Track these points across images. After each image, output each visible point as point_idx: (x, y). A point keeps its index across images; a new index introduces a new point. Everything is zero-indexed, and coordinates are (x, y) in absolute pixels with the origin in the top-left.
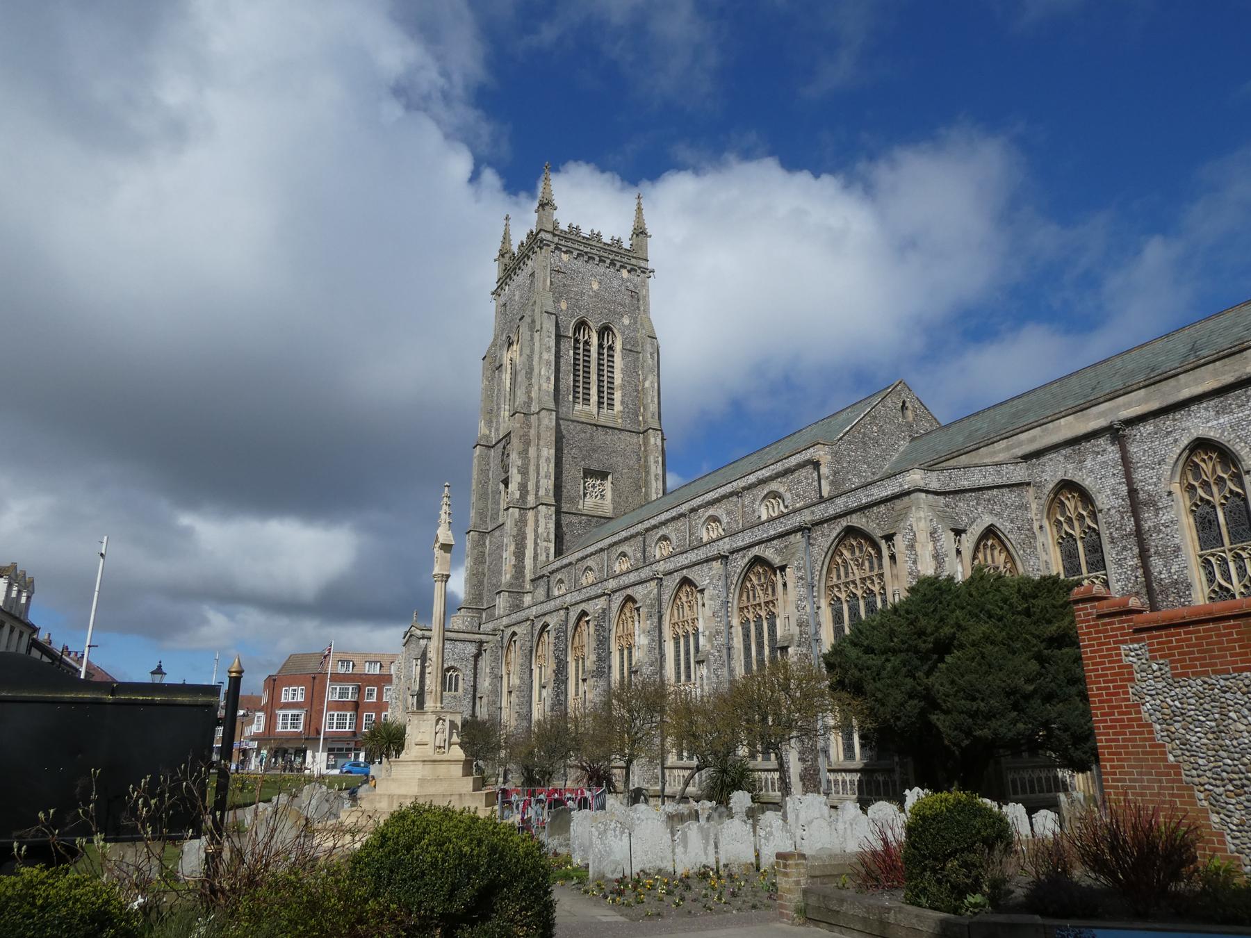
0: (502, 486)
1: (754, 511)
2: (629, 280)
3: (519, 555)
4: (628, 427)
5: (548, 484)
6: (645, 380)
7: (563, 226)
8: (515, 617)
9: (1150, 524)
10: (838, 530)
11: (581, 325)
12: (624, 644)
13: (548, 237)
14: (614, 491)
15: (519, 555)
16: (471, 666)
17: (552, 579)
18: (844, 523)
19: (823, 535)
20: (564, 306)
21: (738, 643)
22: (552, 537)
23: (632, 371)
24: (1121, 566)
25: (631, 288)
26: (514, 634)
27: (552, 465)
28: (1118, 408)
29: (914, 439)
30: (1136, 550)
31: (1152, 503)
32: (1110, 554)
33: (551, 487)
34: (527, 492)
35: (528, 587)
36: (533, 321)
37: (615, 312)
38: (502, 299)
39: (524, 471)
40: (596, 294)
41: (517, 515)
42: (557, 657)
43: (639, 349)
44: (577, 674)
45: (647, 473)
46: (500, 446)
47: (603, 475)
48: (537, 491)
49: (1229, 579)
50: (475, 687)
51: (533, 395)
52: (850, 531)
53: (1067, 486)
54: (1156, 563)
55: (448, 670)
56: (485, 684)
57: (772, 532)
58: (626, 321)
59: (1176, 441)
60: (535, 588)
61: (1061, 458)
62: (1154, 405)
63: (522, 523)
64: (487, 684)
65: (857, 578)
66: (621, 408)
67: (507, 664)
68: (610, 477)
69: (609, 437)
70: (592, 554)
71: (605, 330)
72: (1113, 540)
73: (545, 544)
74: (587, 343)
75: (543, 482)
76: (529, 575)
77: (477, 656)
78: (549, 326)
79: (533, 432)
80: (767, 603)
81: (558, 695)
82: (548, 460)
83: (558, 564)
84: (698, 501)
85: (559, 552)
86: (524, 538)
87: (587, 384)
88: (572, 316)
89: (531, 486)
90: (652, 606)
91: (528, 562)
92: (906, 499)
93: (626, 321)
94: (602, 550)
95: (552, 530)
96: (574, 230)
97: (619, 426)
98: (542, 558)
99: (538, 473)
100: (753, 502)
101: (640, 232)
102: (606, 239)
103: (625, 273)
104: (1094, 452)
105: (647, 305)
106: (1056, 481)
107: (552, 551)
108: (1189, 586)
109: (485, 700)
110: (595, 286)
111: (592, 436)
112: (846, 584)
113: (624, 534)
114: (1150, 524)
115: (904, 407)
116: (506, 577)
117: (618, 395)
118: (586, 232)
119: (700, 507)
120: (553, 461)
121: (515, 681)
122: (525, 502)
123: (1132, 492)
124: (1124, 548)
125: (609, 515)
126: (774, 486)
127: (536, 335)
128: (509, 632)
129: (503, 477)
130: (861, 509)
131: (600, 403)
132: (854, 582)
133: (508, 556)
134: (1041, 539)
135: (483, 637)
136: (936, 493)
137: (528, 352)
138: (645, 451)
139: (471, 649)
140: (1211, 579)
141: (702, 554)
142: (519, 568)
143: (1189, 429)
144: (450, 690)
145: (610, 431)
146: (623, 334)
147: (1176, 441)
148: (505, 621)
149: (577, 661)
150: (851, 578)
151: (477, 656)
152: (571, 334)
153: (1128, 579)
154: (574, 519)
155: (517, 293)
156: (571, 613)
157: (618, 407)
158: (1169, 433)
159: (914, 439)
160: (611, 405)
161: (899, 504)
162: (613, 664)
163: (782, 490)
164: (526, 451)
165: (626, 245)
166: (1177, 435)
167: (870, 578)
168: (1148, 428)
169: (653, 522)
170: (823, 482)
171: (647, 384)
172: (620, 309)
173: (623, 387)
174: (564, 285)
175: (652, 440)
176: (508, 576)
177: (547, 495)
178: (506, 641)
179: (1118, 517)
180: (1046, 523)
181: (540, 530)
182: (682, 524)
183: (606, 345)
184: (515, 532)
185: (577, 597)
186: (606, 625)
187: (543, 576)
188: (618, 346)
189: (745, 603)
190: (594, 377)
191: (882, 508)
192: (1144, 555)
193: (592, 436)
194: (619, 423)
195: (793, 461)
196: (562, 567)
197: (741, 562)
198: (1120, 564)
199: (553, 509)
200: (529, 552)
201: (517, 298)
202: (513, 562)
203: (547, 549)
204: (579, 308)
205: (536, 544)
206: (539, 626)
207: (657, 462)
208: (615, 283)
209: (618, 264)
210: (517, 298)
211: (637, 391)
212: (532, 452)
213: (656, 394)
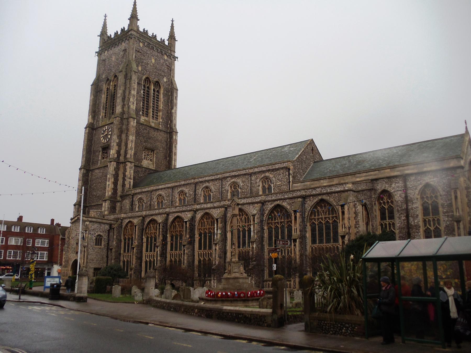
1: (256, 183)
2: (167, 60)
5: (131, 153)
7: (141, 30)
9: (410, 207)
10: (317, 200)
11: (147, 79)
13: (135, 33)
15: (115, 183)
16: (107, 235)
19: (310, 200)
20: (140, 69)
21: (266, 235)
22: (132, 177)
24: (400, 219)
25: (168, 64)
27: (133, 144)
28: (405, 170)
29: (315, 162)
30: (405, 215)
31: (411, 201)
32: (396, 215)
34: (120, 155)
35: (119, 199)
37: (161, 75)
38: (103, 57)
39: (119, 145)
41: (115, 166)
42: (163, 235)
47: (153, 151)
49: (430, 226)
50: (108, 244)
52: (322, 200)
53: (384, 192)
54: (411, 219)
57: (286, 197)
60: (123, 200)
61: (384, 182)
64: (115, 243)
65: (323, 217)
66: (161, 120)
68: (155, 152)
70: (162, 189)
72: (398, 211)
73: (129, 180)
76: (119, 193)
79: (124, 127)
80: (281, 222)
81: (163, 250)
84: (227, 175)
86: (118, 176)
88: (144, 74)
89: (122, 152)
90: (222, 218)
92: (346, 193)
95: (132, 174)
96: (145, 32)
98: (127, 186)
100: (257, 179)
101: (172, 37)
102: (150, 34)
103: (166, 57)
105: (174, 74)
106: (382, 190)
108: (420, 227)
109: (113, 250)
111: (149, 132)
112: (318, 219)
113: (183, 183)
114: (410, 207)
115: (312, 150)
116: (109, 193)
118: (150, 34)
119: (227, 177)
120: (134, 142)
122: (119, 160)
123: (406, 197)
124: (402, 214)
126: (267, 174)
128: (127, 221)
130: (328, 194)
132: (322, 218)
134: (374, 207)
135: (112, 222)
136: (355, 191)
139: (107, 227)
140: (425, 225)
141: (249, 200)
143: (425, 180)
149: (172, 237)
150: (320, 217)
153: (402, 223)
154: (139, 169)
158: (419, 181)
159: (315, 162)
161: (344, 195)
163: (271, 176)
165: (167, 43)
166: (421, 181)
167: (328, 217)
169: (201, 180)
170: (291, 176)
176: (110, 193)
177: (131, 158)
179: (400, 204)
180: (377, 203)
181: (127, 173)
182: (218, 184)
184: (114, 173)
185: (173, 210)
186: (193, 223)
188: (162, 91)
189: (270, 222)
191: (336, 195)
192: (407, 217)
193: (149, 132)
195: (277, 166)
197: (270, 206)
198: (399, 218)
199: (133, 164)
202: (113, 187)
203: (130, 182)
204: (146, 71)
206: (148, 220)
208: (162, 61)
209: (163, 52)
211: (168, 113)
212: (124, 136)
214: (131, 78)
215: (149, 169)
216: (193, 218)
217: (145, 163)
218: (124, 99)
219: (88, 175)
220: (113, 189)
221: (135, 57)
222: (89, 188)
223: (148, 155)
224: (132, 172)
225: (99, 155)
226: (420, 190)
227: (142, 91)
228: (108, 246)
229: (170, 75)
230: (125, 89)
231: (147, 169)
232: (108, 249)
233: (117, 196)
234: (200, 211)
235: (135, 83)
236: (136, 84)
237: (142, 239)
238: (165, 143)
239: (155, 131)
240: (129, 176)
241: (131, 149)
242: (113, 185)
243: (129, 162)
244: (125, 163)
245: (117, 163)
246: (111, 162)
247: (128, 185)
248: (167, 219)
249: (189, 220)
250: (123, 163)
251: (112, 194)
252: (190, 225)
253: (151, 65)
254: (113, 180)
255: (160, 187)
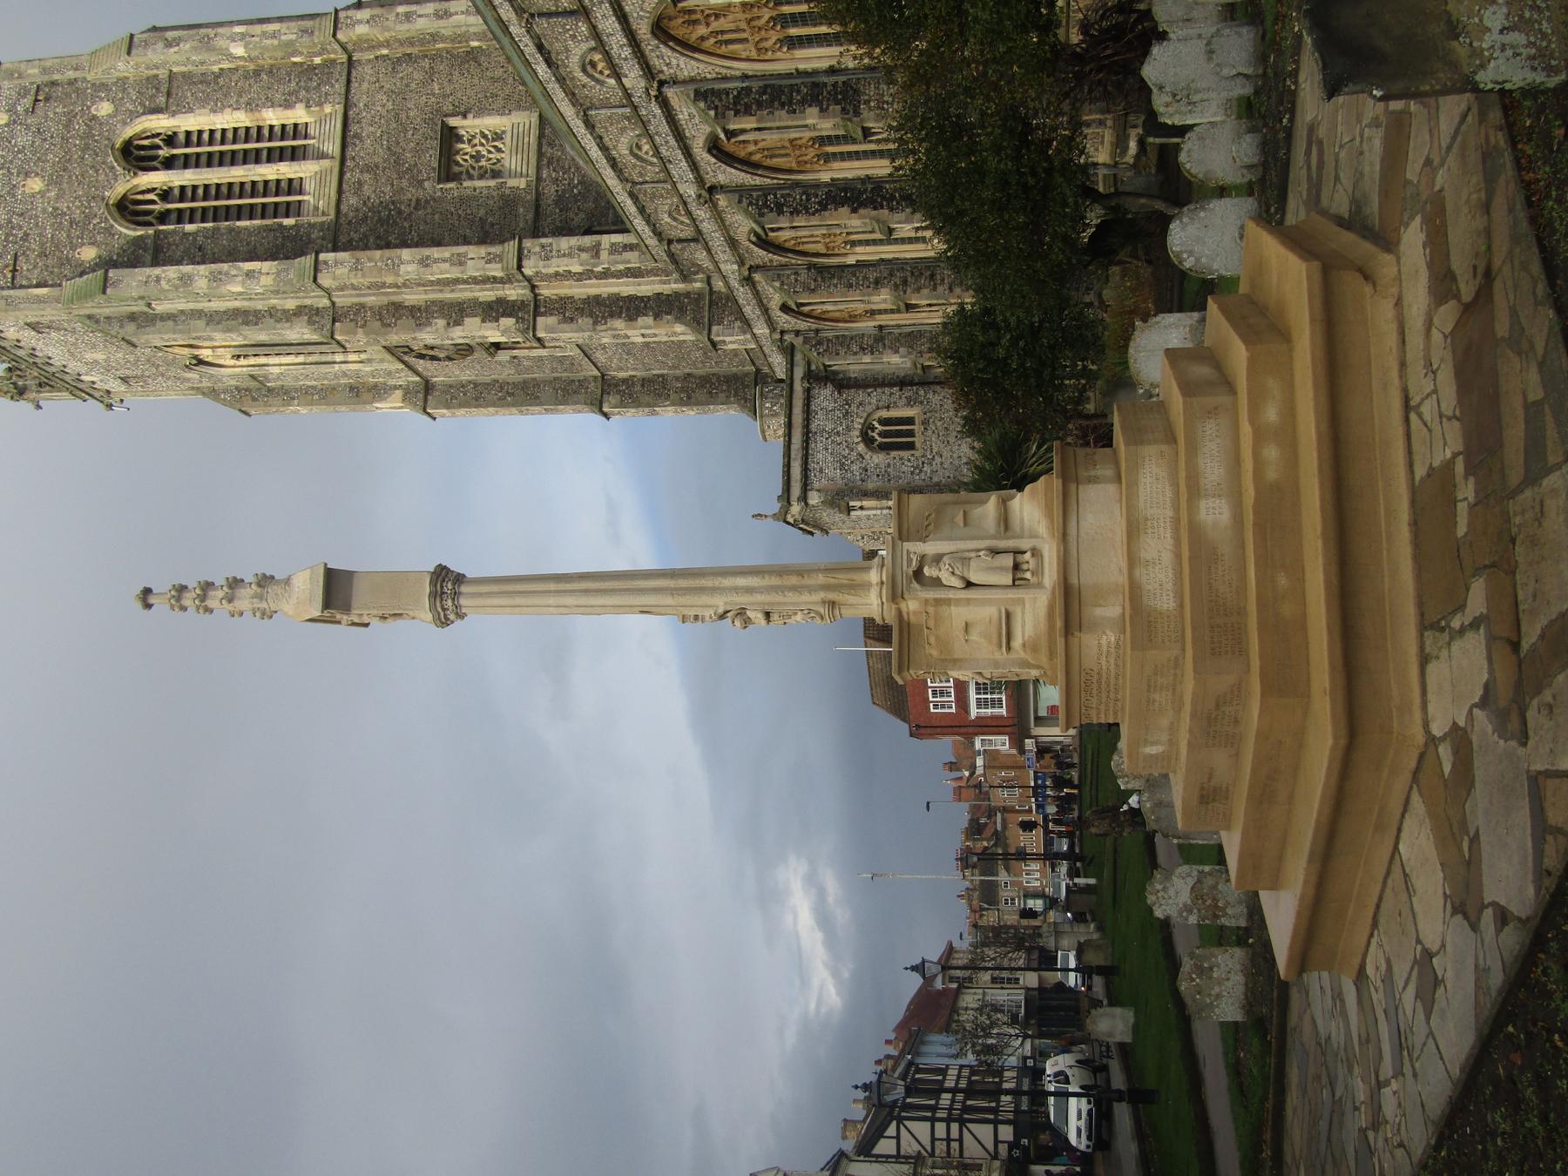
0: (503, 356)
3: (631, 308)
4: (340, 87)
5: (476, 261)
6: (233, 58)
8: (750, 310)
12: (774, 36)
14: (480, 113)
15: (631, 308)
16: (860, 395)
17: (675, 234)
22: (588, 240)
23: (214, 87)
25: (27, 102)
26: (785, 308)
27: (436, 252)
33: (482, 250)
34: (501, 301)
36: (132, 317)
37: (88, 135)
38: (115, 386)
39: (457, 313)
40: (52, 182)
41: (551, 320)
43: (163, 73)
44: (857, 156)
45: (435, 37)
46: (420, 365)
47: (449, 137)
48: (495, 280)
50: (903, 382)
51: (291, 304)
55: (868, 441)
56: (896, 361)
58: (104, 109)
60: (700, 269)
63: (567, 310)
67: (853, 318)
68: (453, 122)
69: (367, 129)
70: (604, 148)
71: (136, 156)
73: (604, 255)
74: (165, 195)
75: (473, 269)
76: (674, 286)
77: (842, 383)
78: (133, 283)
82: (425, 263)
83: (639, 223)
85: (621, 226)
86: (596, 301)
87: (253, 188)
88: (109, 231)
89: (487, 294)
91: (646, 288)
93: (104, 109)
94: (590, 125)
95: (574, 241)
97: (340, 108)
98: (633, 259)
99: (456, 281)
107: (617, 238)
110: (35, 185)
111: (367, 169)
113: (542, 69)
116: (681, 332)
117: (273, 117)
120: (426, 251)
121: (883, 298)
125: (535, 119)
127: (160, 308)
128: (783, 320)
129: (479, 354)
131: (294, 155)
133: (640, 332)
135: (799, 372)
137: (201, 323)
138: (387, 44)
139: (825, 397)
142: (662, 306)
144: (911, 434)
145: (354, 128)
146: (133, 115)
148: (761, 329)
149: (829, 158)
151: (842, 383)
152: (151, 231)
155: (89, 356)
156: (722, 178)
157: (299, 115)
160: (297, 131)
162: (824, 65)
164: (414, 311)
171: (238, 50)
172: (79, 126)
173: (251, 106)
174: (43, 255)
175: (362, 30)
176: (679, 328)
177: (498, 258)
178: (802, 325)
181: (577, 268)
183: (164, 152)
184: (584, 321)
185: (680, 168)
187: (671, 255)
188: (161, 123)
190: (237, 174)
193: (367, 169)
194: (332, 109)
196: (642, 210)
199: (527, 243)
200: (626, 288)
201: (100, 356)
202: (649, 320)
203: (614, 249)
204: (88, 218)
205: (606, 274)
206: (761, 255)
207: (408, 17)
210: (100, 356)
211: (257, 73)
212: (412, 298)
213: (258, 29)
214: (142, 298)
215: (540, 145)
216: (705, 94)
217: (518, 169)
218: (246, 313)
219: (625, 381)
220: (657, 317)
221: (38, 286)
222: (678, 372)
223: (477, 157)
224: (565, 243)
225: (528, 358)
227: (189, 228)
228: (912, 384)
229: (72, 82)
230: (197, 314)
231: (540, 154)
232: (922, 384)
233: (687, 295)
234: (656, 63)
235: (158, 279)
236: (157, 271)
237: (860, 265)
238: (406, 70)
239: (357, 136)
240: (584, 256)
241: (460, 261)
242: (641, 321)
243: (520, 267)
244: (528, 279)
245: (536, 314)
246: (539, 340)
247: (628, 255)
248: (740, 192)
249: (720, 116)
250: (533, 287)
251: (678, 319)
252: (748, 111)
253: (58, 197)
254: (619, 324)
255: (595, 152)
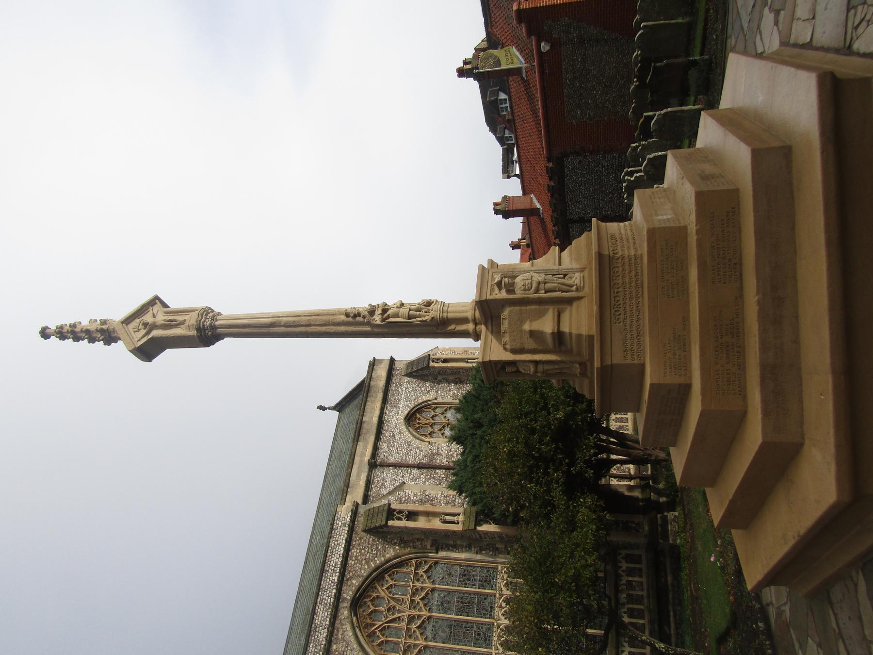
18: (345, 613)
28: (361, 461)
59: (400, 432)
62: (372, 439)
104: (381, 487)
147: (400, 432)
166: (396, 431)
168: (384, 446)
191: (354, 552)
226: (412, 434)
